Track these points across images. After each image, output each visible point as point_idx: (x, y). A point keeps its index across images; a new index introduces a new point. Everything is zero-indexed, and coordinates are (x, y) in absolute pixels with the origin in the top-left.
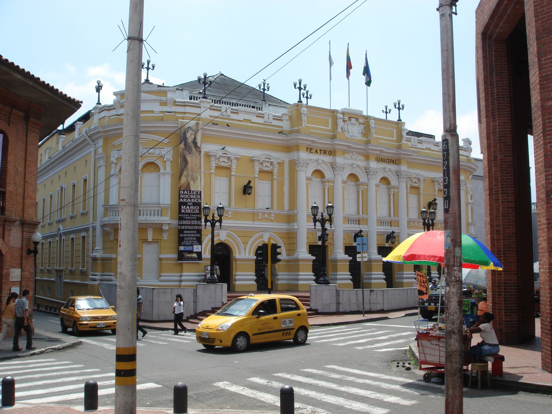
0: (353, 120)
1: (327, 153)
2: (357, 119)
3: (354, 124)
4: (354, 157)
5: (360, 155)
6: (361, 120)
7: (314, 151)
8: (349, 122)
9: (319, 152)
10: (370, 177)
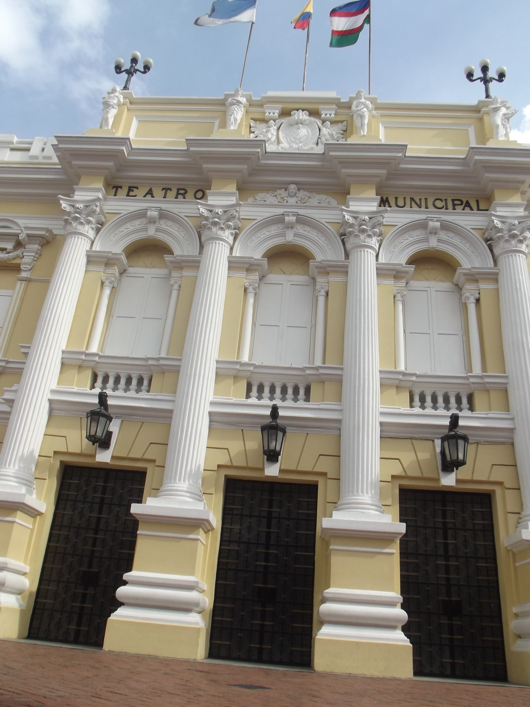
1: (190, 195)
2: (314, 113)
4: (292, 201)
6: (328, 113)
7: (140, 192)
8: (285, 120)
9: (158, 193)
10: (350, 242)
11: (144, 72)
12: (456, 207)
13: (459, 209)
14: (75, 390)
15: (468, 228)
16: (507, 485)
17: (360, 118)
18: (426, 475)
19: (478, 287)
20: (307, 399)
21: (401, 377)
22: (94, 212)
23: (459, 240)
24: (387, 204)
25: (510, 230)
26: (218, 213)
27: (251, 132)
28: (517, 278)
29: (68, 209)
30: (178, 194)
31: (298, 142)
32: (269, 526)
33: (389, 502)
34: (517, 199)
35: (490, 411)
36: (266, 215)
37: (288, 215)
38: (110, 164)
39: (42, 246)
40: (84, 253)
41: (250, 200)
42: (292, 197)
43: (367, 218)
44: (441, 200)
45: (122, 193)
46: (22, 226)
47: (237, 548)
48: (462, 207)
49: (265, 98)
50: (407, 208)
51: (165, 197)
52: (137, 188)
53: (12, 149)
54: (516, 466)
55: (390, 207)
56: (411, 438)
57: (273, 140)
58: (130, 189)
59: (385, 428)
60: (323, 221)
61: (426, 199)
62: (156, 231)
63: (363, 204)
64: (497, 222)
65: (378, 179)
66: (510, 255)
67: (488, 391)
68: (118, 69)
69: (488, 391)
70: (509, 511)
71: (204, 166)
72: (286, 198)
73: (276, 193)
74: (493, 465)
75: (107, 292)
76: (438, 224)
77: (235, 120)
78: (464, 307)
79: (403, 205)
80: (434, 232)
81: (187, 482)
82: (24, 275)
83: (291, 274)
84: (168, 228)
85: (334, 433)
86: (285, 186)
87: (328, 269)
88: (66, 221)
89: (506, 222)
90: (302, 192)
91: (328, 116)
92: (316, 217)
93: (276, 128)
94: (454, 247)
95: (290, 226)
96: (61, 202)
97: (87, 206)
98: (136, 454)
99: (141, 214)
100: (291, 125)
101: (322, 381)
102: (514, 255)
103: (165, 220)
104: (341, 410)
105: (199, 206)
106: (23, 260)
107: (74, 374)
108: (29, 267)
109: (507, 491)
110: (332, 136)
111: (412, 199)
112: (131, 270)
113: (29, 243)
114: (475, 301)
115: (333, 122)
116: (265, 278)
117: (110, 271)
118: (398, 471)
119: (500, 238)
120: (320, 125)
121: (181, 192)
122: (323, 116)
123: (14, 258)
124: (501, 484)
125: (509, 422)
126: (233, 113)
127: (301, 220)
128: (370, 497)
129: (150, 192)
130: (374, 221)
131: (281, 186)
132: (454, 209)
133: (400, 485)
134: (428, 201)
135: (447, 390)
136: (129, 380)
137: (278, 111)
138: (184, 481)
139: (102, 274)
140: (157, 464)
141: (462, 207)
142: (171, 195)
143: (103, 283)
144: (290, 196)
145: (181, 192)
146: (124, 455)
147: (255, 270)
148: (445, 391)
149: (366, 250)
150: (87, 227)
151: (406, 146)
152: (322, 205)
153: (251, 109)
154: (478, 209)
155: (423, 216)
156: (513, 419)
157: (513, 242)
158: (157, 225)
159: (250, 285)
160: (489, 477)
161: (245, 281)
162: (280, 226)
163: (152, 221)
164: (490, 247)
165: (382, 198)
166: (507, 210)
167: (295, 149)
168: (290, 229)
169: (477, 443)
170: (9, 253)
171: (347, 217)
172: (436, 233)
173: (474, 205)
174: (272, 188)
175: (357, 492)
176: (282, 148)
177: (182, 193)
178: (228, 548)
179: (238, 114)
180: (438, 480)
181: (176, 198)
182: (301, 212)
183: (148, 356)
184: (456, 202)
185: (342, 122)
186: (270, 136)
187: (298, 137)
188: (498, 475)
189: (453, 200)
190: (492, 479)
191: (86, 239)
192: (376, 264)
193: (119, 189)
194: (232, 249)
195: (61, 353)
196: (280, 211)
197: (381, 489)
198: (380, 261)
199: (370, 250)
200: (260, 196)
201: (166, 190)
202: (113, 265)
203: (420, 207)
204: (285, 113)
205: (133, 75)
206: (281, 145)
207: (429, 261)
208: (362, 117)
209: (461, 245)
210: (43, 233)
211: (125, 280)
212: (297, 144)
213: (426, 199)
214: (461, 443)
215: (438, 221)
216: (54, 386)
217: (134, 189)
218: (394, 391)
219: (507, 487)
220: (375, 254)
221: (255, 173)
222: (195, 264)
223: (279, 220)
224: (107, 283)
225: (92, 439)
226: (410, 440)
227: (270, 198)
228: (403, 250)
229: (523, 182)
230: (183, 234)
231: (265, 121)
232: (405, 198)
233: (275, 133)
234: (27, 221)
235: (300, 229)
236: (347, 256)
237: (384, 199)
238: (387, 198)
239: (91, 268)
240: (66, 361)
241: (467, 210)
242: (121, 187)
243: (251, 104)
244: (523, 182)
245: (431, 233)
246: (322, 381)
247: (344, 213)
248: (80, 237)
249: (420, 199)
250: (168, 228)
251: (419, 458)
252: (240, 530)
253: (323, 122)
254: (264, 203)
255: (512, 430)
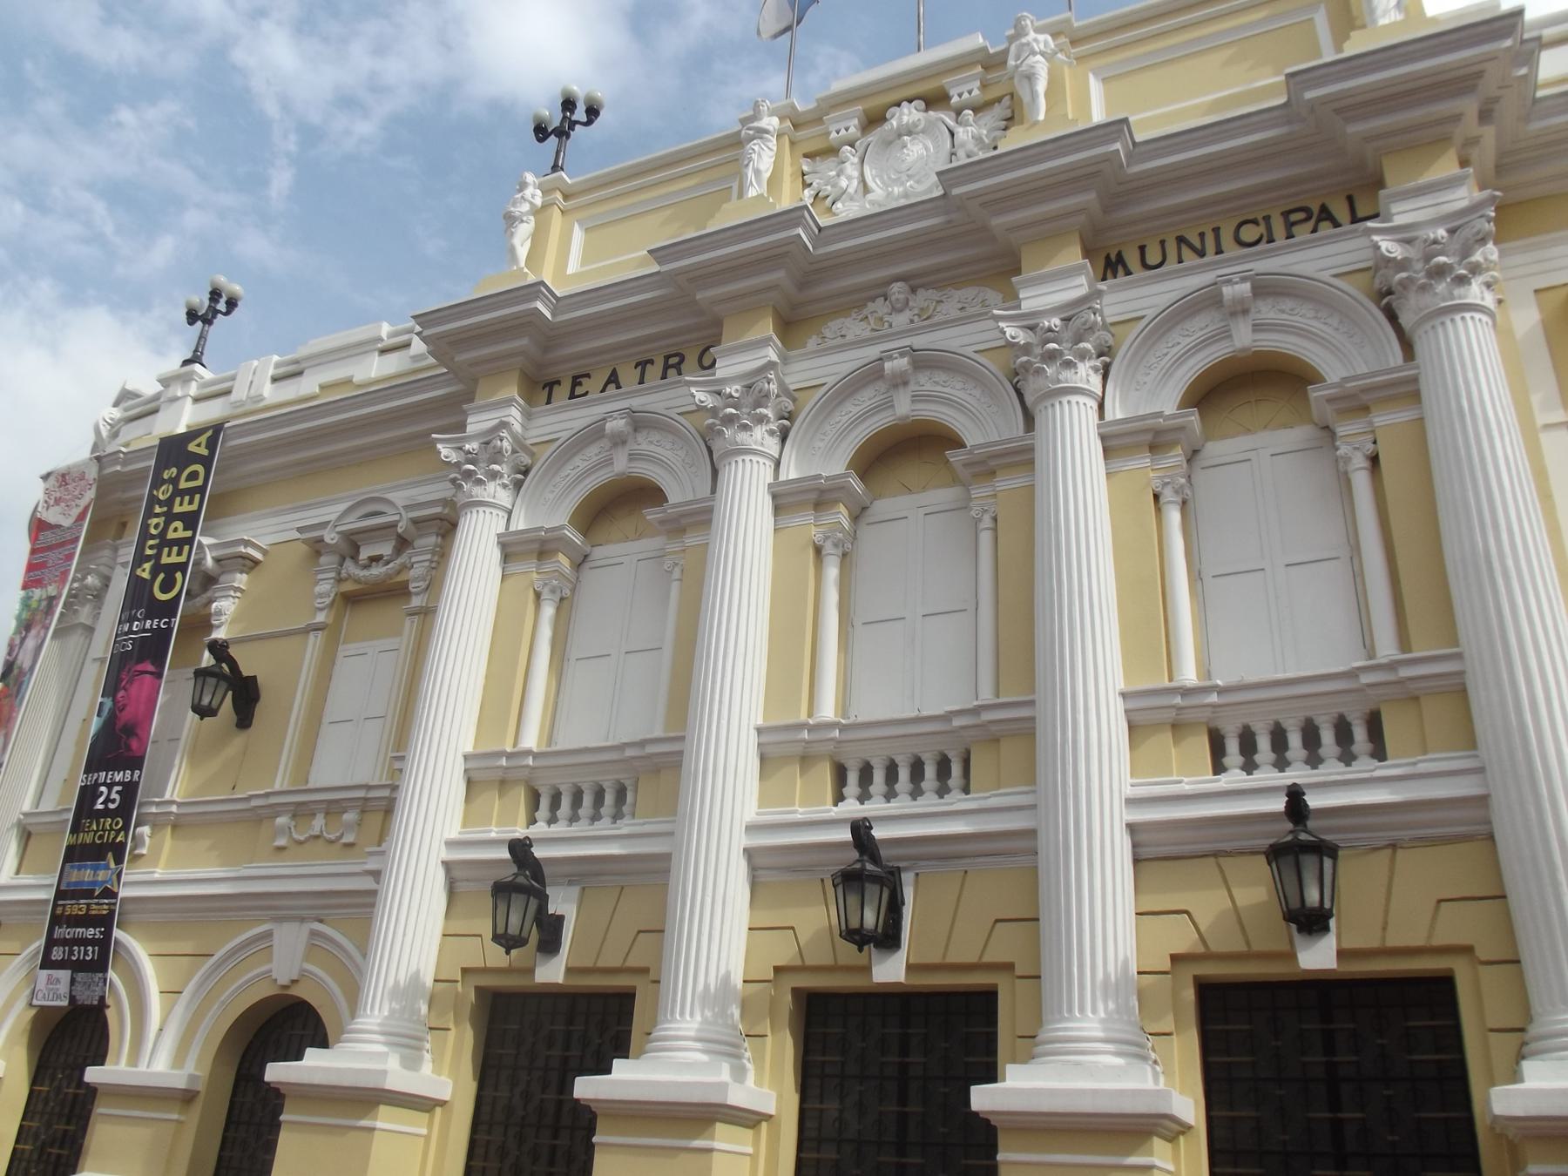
0: (909, 114)
2: (936, 100)
3: (910, 131)
4: (900, 320)
5: (957, 283)
6: (965, 89)
8: (874, 137)
9: (628, 375)
11: (589, 123)
12: (1295, 229)
13: (1303, 233)
14: (493, 835)
15: (1325, 276)
16: (1482, 953)
17: (1025, 82)
18: (1257, 947)
19: (1371, 423)
20: (966, 790)
21: (1178, 700)
22: (500, 451)
23: (1311, 314)
24: (1120, 268)
25: (1428, 258)
26: (731, 396)
27: (806, 185)
28: (1460, 380)
29: (454, 457)
30: (666, 367)
31: (904, 178)
32: (903, 1099)
33: (1167, 1024)
34: (1446, 166)
35: (1425, 752)
36: (846, 368)
37: (891, 358)
38: (523, 342)
39: (443, 537)
40: (493, 540)
41: (812, 343)
42: (901, 311)
43: (1056, 321)
44: (1255, 222)
45: (562, 391)
46: (400, 503)
47: (834, 1156)
48: (1311, 224)
49: (823, 100)
50: (1171, 265)
51: (641, 382)
52: (588, 376)
53: (383, 352)
54: (1504, 897)
55: (1128, 273)
56: (1216, 854)
57: (851, 190)
58: (576, 382)
59: (1142, 837)
60: (969, 351)
61: (1216, 231)
62: (630, 460)
63: (1056, 286)
64: (1389, 247)
65: (1082, 218)
66: (1437, 322)
67: (1416, 699)
68: (541, 132)
69: (1416, 699)
70: (1491, 1025)
71: (698, 297)
72: (886, 318)
73: (865, 312)
74: (1440, 901)
75: (548, 611)
76: (1247, 286)
77: (757, 172)
78: (1345, 482)
79: (1159, 260)
80: (1240, 310)
81: (698, 1018)
82: (416, 602)
83: (924, 489)
84: (652, 448)
85: (1019, 864)
86: (879, 291)
87: (993, 463)
88: (453, 481)
89: (1416, 238)
90: (921, 293)
91: (966, 95)
92: (953, 345)
93: (856, 160)
94: (1299, 335)
95: (900, 381)
96: (439, 446)
97: (487, 443)
98: (611, 959)
99: (595, 433)
100: (887, 144)
101: (993, 739)
102: (1448, 323)
103: (645, 433)
104: (1034, 807)
105: (693, 390)
106: (412, 573)
107: (493, 802)
108: (423, 585)
109: (1482, 969)
110: (978, 139)
111: (1181, 240)
112: (598, 553)
113: (421, 536)
114: (1366, 464)
115: (977, 109)
116: (868, 512)
117: (548, 567)
118: (1184, 940)
119: (1404, 284)
120: (951, 123)
121: (673, 361)
122: (955, 99)
123: (399, 572)
124: (1467, 950)
125: (1474, 779)
126: (751, 159)
127: (924, 362)
128: (1102, 1021)
129: (613, 379)
130: (1076, 324)
131: (872, 293)
132: (1290, 236)
133: (1196, 978)
134: (1222, 232)
135: (1308, 714)
136: (599, 796)
137: (856, 121)
138: (692, 1015)
139: (535, 575)
140: (652, 976)
141: (1311, 224)
142: (654, 371)
143: (538, 595)
144: (896, 310)
145: (673, 361)
146: (588, 963)
147: (836, 502)
148: (1302, 715)
149: (1065, 400)
150: (492, 486)
151: (1125, 121)
152: (971, 311)
153: (801, 134)
154: (1355, 220)
155: (1208, 277)
156: (1480, 770)
157: (1441, 287)
158: (631, 446)
159: (826, 538)
160: (1430, 936)
161: (813, 530)
162: (881, 386)
163: (619, 441)
164: (1392, 317)
165: (1108, 257)
166: (1430, 200)
167: (899, 197)
168: (901, 390)
169: (1393, 846)
170: (388, 563)
171: (1010, 331)
172: (1245, 312)
173: (1340, 211)
174: (855, 302)
175: (1070, 1010)
176: (872, 203)
177: (674, 364)
178: (815, 1155)
179: (763, 158)
180: (1291, 956)
181: (664, 377)
182: (919, 341)
183: (625, 740)
184: (1294, 217)
185: (999, 100)
186: (843, 183)
187: (904, 167)
188: (1455, 927)
189: (1286, 214)
190: (1438, 941)
191: (495, 512)
192: (1099, 426)
193: (556, 388)
194: (778, 464)
195: (461, 760)
196: (873, 352)
197: (1141, 995)
198: (1109, 416)
199: (1082, 399)
200: (832, 328)
201: (643, 365)
202: (555, 552)
203: (1201, 254)
204: (874, 120)
205: (568, 136)
206: (869, 197)
207: (1244, 386)
208: (1030, 77)
209: (1316, 326)
210: (438, 510)
211: (589, 576)
212: (903, 184)
213: (1216, 231)
214: (1309, 862)
215: (1244, 280)
216: (454, 832)
217: (584, 380)
218: (1167, 737)
219: (1483, 958)
220: (1095, 406)
221: (804, 283)
222: (701, 518)
223: (871, 374)
224: (546, 595)
225: (507, 941)
226: (1212, 860)
227: (854, 327)
228: (1168, 374)
229: (1456, 118)
230: (682, 453)
231: (832, 151)
232: (1162, 243)
233: (856, 174)
234: (406, 495)
235: (926, 382)
236: (1029, 420)
237: (1113, 257)
238: (1119, 255)
239: (513, 568)
240: (476, 776)
241: (1326, 229)
242: (558, 382)
243: (798, 122)
244: (1456, 118)
245: (1233, 314)
246: (993, 739)
247: (1002, 324)
248: (481, 509)
249: (1202, 235)
250: (652, 448)
251: (1239, 903)
252: (841, 1111)
253: (958, 112)
254: (840, 341)
255: (1483, 801)
